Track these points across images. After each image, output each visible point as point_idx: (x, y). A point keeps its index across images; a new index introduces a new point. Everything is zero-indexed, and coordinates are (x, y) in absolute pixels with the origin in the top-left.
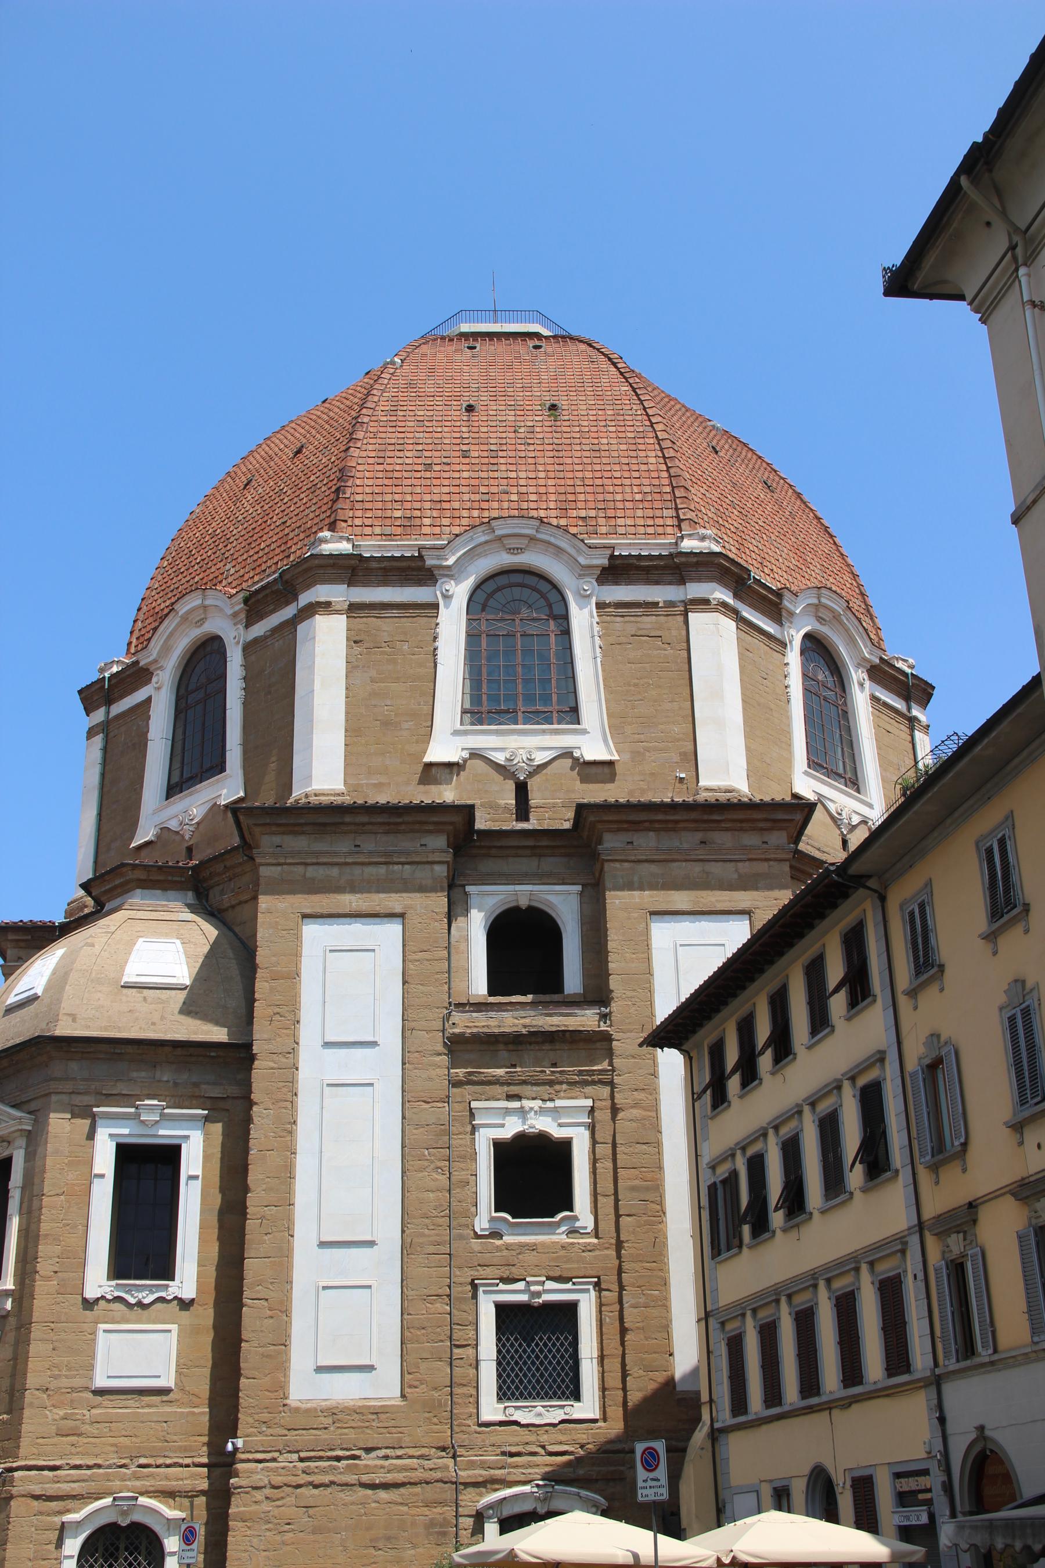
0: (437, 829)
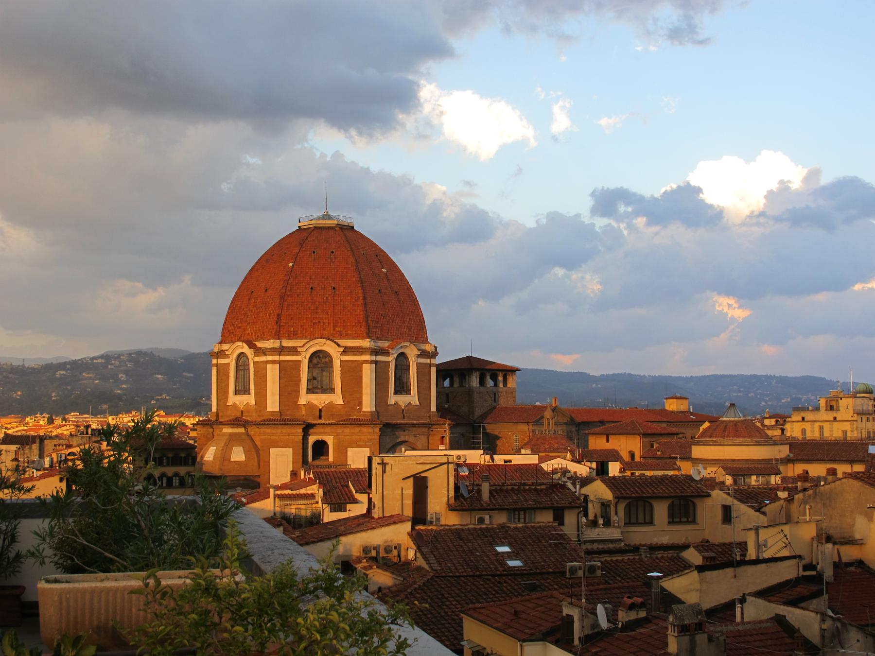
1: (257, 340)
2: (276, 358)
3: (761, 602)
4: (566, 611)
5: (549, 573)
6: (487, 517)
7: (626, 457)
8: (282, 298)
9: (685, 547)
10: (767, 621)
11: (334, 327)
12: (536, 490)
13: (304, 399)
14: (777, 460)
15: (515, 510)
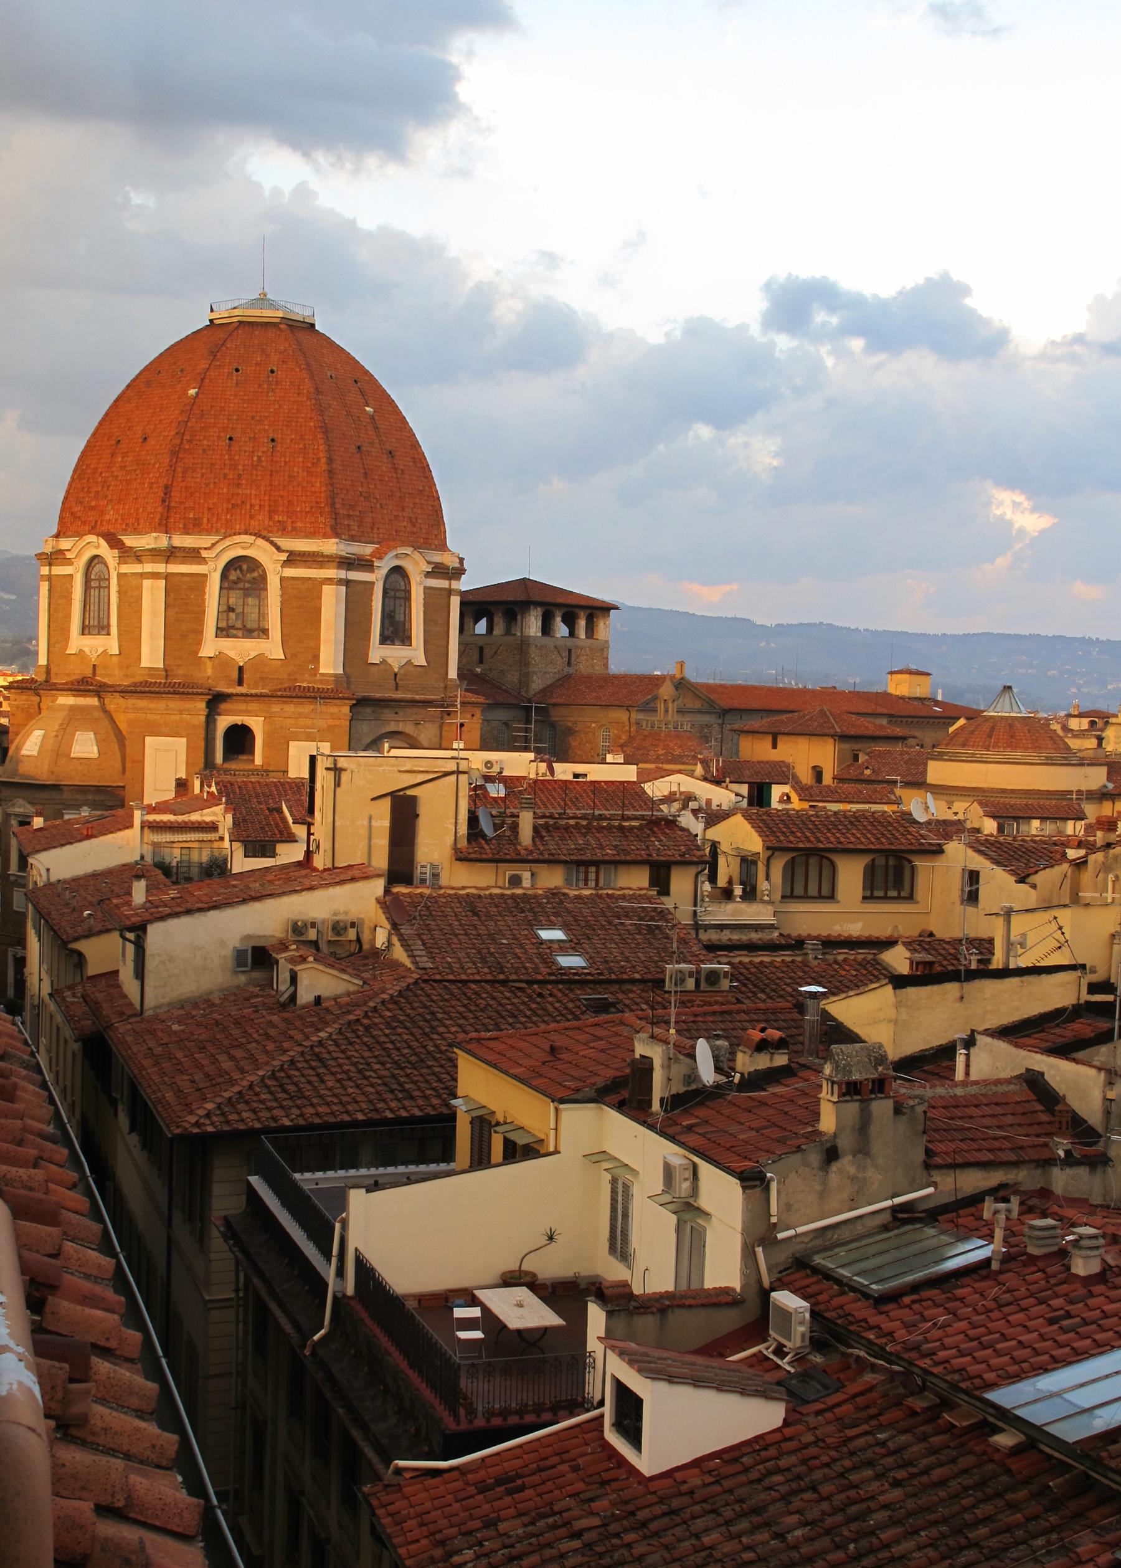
0: (202, 700)
1: (125, 532)
2: (161, 568)
3: (1001, 1046)
4: (641, 1049)
5: (633, 981)
6: (526, 876)
7: (806, 777)
8: (175, 453)
9: (889, 943)
10: (1008, 1081)
11: (272, 513)
12: (621, 828)
13: (211, 646)
14: (1079, 792)
15: (579, 863)
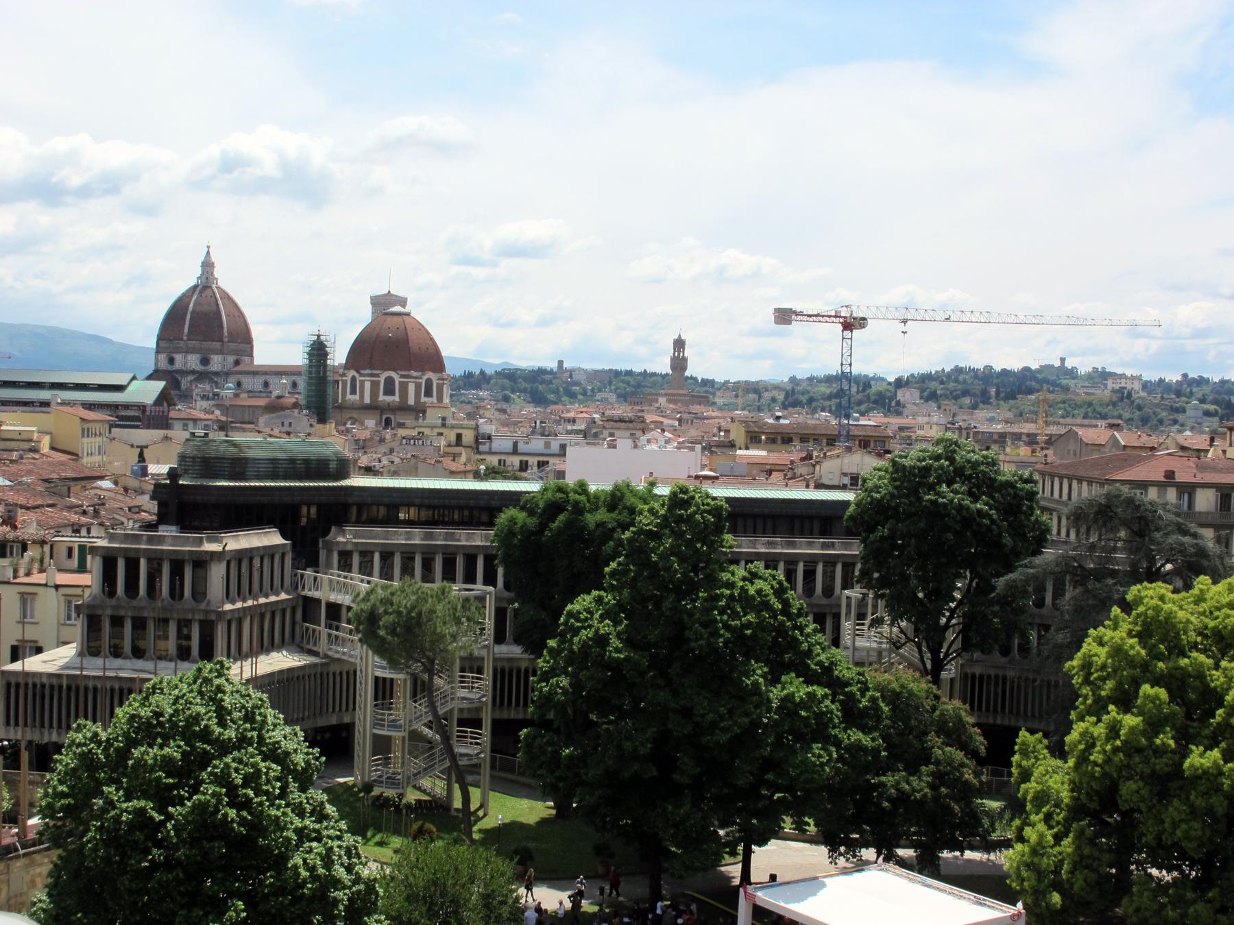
13: (382, 398)
